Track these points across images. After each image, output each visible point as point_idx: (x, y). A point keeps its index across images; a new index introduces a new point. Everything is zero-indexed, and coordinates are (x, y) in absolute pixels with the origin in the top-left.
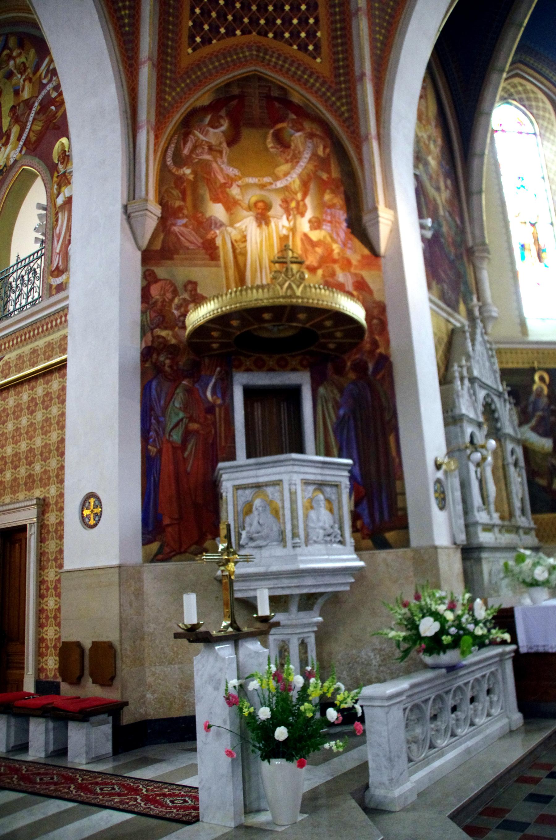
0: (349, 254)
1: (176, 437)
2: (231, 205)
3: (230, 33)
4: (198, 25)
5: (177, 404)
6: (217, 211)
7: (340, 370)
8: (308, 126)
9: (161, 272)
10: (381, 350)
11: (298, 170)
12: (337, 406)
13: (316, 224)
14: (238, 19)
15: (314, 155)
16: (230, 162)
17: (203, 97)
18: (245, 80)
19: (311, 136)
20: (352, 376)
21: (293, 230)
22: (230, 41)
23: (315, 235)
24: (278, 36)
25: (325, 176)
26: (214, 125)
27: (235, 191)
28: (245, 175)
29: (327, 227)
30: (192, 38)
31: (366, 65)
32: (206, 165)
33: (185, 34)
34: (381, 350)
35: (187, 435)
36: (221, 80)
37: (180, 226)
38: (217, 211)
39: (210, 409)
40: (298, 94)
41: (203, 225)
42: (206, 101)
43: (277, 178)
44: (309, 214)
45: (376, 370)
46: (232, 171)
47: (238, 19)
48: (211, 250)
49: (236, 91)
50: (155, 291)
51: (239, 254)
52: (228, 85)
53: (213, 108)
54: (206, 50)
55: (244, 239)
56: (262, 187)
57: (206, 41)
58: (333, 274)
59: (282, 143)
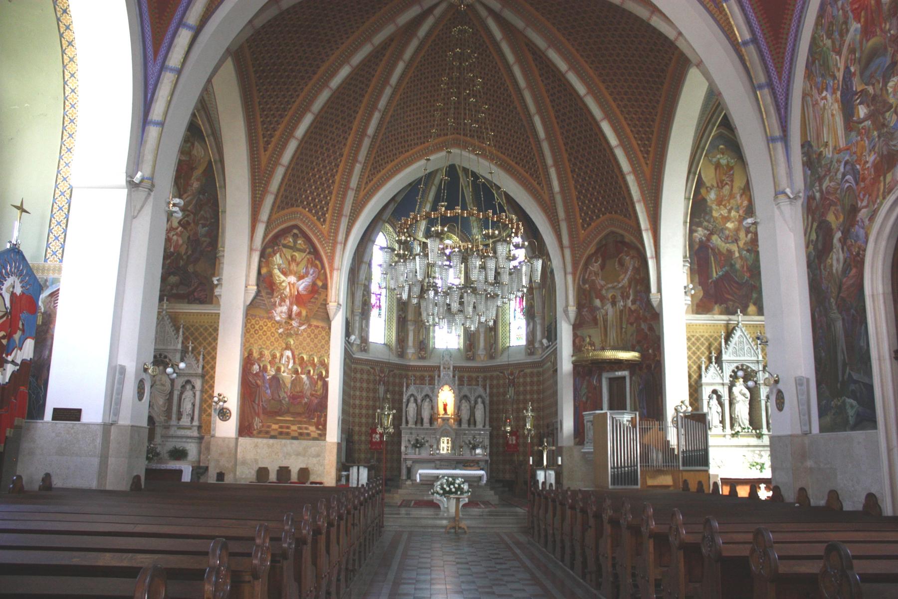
0: (646, 314)
1: (584, 399)
2: (602, 299)
3: (598, 217)
4: (584, 220)
5: (584, 386)
6: (598, 302)
7: (641, 369)
8: (632, 253)
9: (579, 333)
10: (657, 358)
11: (628, 276)
12: (639, 385)
13: (633, 302)
14: (600, 210)
15: (634, 267)
16: (602, 279)
17: (591, 249)
18: (608, 235)
19: (633, 258)
20: (645, 371)
21: (625, 306)
22: (599, 221)
23: (633, 308)
24: (616, 212)
25: (638, 277)
26: (596, 262)
27: (604, 292)
28: (608, 283)
29: (638, 303)
30: (583, 226)
31: (644, 223)
32: (593, 281)
33: (580, 226)
34: (657, 358)
35: (587, 399)
36: (598, 239)
37: (585, 312)
38: (598, 302)
39: (595, 388)
40: (628, 237)
41: (593, 309)
42: (593, 251)
43: (619, 283)
44: (631, 298)
45: (655, 368)
46: (603, 283)
47: (600, 210)
48: (595, 321)
49: (604, 242)
50: (577, 341)
51: (605, 321)
52: (601, 240)
53: (595, 253)
54: (590, 228)
55: (607, 314)
56: (613, 288)
57: (589, 225)
58: (640, 325)
59: (621, 264)
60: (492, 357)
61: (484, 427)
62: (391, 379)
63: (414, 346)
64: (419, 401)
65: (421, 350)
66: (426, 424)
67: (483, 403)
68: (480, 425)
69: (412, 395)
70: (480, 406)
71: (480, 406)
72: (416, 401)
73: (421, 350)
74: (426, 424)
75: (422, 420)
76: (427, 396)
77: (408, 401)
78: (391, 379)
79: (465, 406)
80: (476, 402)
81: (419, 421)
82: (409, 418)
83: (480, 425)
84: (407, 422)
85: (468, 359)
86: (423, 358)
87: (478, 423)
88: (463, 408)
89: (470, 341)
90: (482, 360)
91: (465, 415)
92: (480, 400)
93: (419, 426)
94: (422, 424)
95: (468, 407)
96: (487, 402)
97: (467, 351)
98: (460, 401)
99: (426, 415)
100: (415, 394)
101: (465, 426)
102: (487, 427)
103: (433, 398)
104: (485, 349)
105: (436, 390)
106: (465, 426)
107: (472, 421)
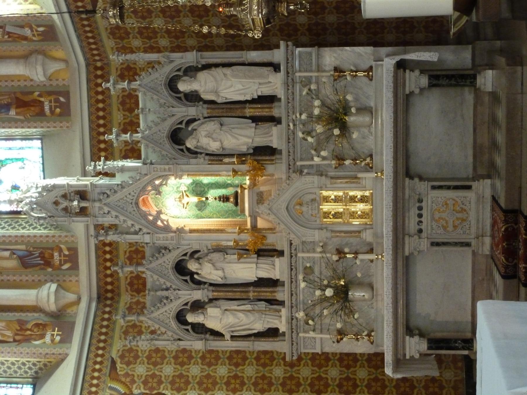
60: (49, 33)
61: (276, 67)
62: (141, 370)
63: (36, 285)
64: (198, 295)
65: (48, 263)
66: (276, 269)
67: (191, 71)
68: (273, 84)
69: (180, 318)
70: (204, 84)
71: (204, 84)
72: (197, 306)
73: (48, 263)
74: (276, 269)
75: (261, 283)
76: (180, 268)
77: (200, 329)
78: (141, 370)
79: (207, 136)
80: (193, 98)
81: (266, 293)
82: (259, 326)
83: (273, 84)
84: (272, 333)
85: (64, 111)
86: (72, 257)
87: (266, 91)
88: (214, 146)
89: (7, 107)
90: (66, 65)
91: (241, 136)
92: (183, 87)
93: (282, 294)
94: (273, 283)
95: (212, 126)
96: (190, 58)
97: (41, 113)
98: (194, 153)
99: (246, 271)
100: (174, 307)
101: (274, 136)
102: (278, 56)
103: (187, 247)
104: (25, 57)
105: (161, 239)
106: (274, 136)
107: (261, 110)
